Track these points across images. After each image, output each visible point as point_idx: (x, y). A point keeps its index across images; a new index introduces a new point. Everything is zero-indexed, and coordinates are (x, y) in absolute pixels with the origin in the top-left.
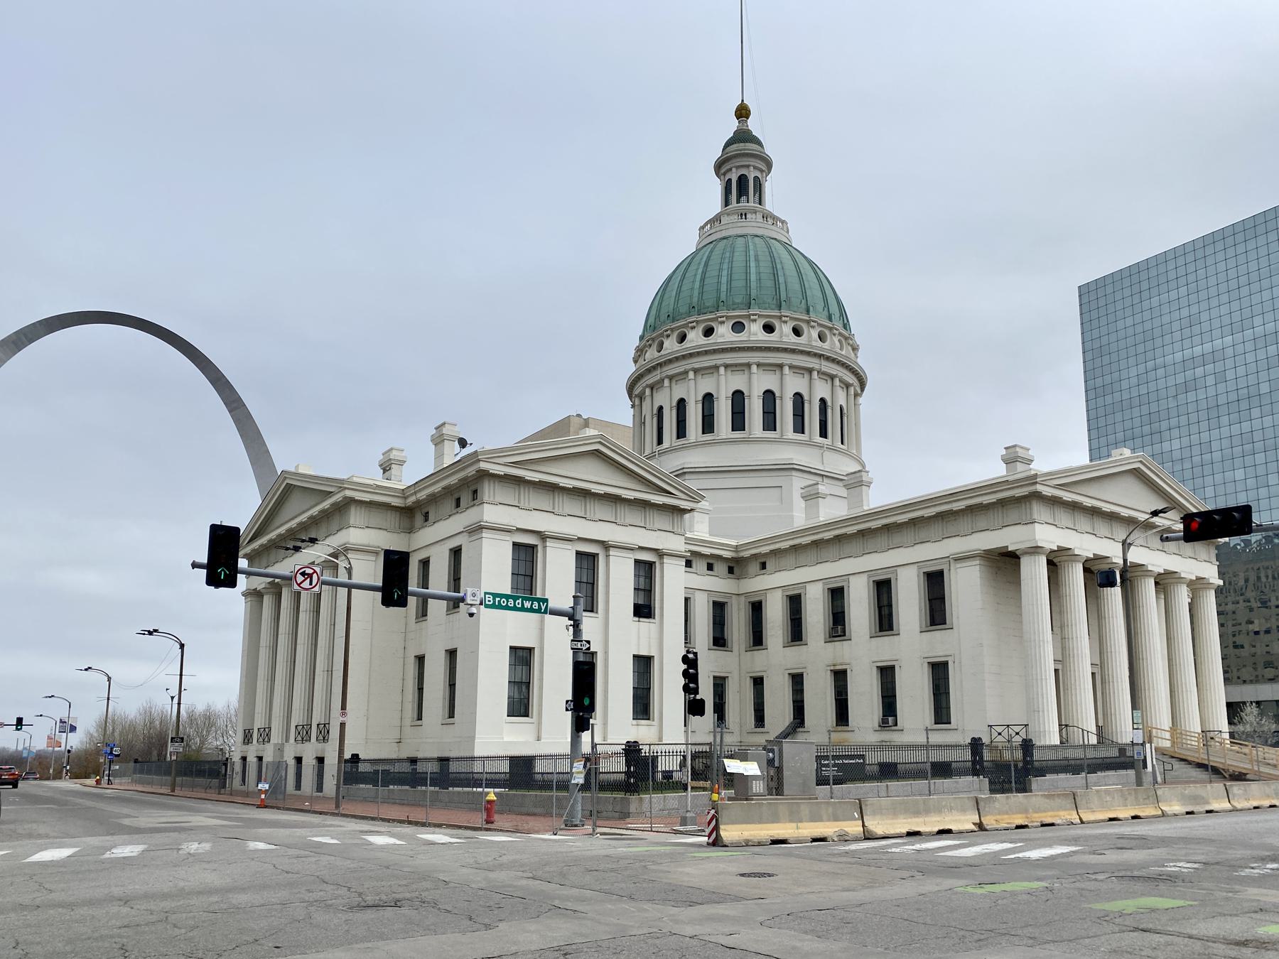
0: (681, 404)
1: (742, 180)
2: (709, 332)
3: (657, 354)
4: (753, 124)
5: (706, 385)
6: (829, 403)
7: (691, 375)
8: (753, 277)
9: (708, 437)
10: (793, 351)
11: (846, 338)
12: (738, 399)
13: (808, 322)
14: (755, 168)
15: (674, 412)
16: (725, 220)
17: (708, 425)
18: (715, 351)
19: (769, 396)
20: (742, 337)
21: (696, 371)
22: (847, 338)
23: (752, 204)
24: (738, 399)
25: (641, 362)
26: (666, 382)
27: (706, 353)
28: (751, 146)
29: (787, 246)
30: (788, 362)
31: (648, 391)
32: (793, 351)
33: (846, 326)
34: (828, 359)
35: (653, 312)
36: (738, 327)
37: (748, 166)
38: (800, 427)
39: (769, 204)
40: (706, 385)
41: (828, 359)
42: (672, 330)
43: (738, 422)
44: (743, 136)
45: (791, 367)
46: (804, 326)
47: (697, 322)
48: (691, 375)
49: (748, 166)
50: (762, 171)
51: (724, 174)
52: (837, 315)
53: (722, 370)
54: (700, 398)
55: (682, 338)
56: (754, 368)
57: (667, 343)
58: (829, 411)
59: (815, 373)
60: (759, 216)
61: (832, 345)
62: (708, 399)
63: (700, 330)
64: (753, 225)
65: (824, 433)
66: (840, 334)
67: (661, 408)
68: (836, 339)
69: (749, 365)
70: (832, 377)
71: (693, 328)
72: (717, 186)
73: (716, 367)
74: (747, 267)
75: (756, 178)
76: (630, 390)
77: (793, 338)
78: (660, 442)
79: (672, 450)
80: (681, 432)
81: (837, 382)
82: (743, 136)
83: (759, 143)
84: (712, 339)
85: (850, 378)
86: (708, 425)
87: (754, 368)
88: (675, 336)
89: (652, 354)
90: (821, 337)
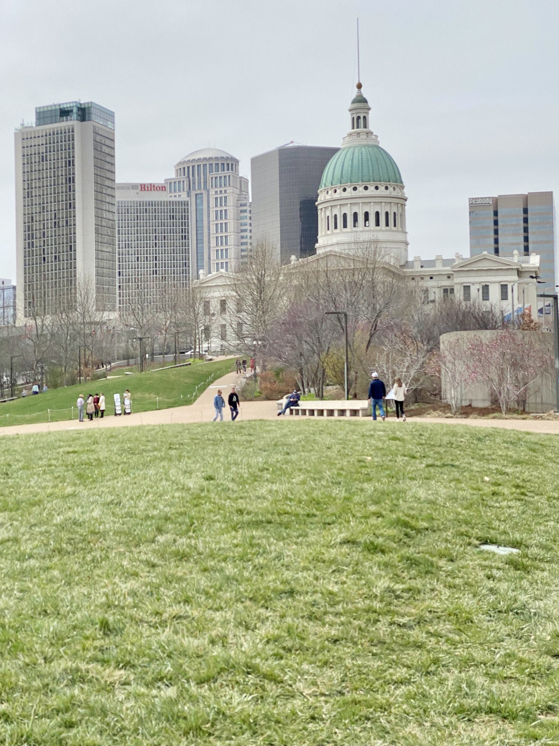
1: (359, 118)
19: (367, 215)
21: (340, 205)
23: (362, 129)
24: (355, 215)
36: (355, 189)
45: (374, 202)
55: (335, 191)
57: (330, 192)
62: (345, 215)
63: (342, 188)
65: (387, 225)
75: (364, 117)
80: (336, 227)
83: (365, 101)
90: (387, 188)
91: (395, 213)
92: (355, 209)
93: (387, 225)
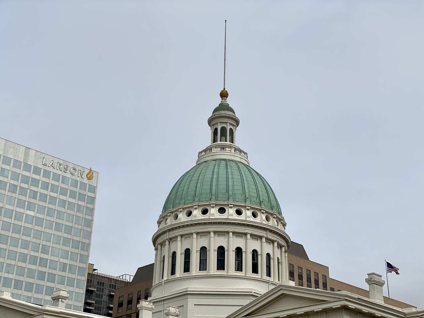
0: (187, 253)
1: (223, 130)
2: (205, 212)
3: (174, 222)
4: (229, 101)
5: (203, 242)
6: (272, 257)
7: (195, 236)
8: (230, 184)
9: (203, 273)
10: (253, 226)
11: (280, 220)
12: (221, 251)
13: (260, 210)
14: (230, 124)
15: (183, 256)
16: (214, 150)
17: (203, 265)
18: (210, 223)
19: (239, 251)
20: (224, 216)
21: (197, 233)
22: (281, 220)
23: (228, 143)
24: (221, 251)
25: (161, 227)
26: (179, 238)
27: (205, 224)
28: (230, 113)
29: (247, 167)
30: (250, 232)
31: (167, 243)
32: (253, 226)
33: (280, 213)
34: (271, 231)
35: (172, 197)
36: (222, 210)
37: (226, 123)
38: (255, 270)
39: (238, 143)
40: (203, 242)
41: (271, 231)
42: (184, 209)
43: (221, 265)
44: (223, 107)
45: (252, 235)
46: (259, 213)
47: (199, 206)
48: (195, 236)
49: (226, 123)
50: (233, 125)
51: (213, 125)
52: (275, 207)
53: (212, 234)
54: (199, 250)
55: (189, 214)
56: (231, 234)
57: (180, 215)
58: (272, 261)
59: (264, 240)
60: (233, 150)
61: (273, 223)
62: (203, 250)
64: (228, 154)
65: (269, 275)
66: (277, 217)
67: (174, 253)
68: (275, 220)
69: (228, 232)
70: (273, 242)
71: (196, 209)
72: (209, 132)
73: (209, 232)
74: (227, 178)
75: (231, 130)
76: (155, 240)
77: (252, 219)
78: (173, 272)
79: (181, 279)
80: (187, 269)
81: (276, 244)
82: (223, 107)
84: (206, 216)
85: (283, 243)
86: (203, 265)
87: (231, 234)
88: (185, 211)
89: (170, 221)
90: (267, 219)
91: (278, 258)
92: (221, 241)
93: (269, 275)
